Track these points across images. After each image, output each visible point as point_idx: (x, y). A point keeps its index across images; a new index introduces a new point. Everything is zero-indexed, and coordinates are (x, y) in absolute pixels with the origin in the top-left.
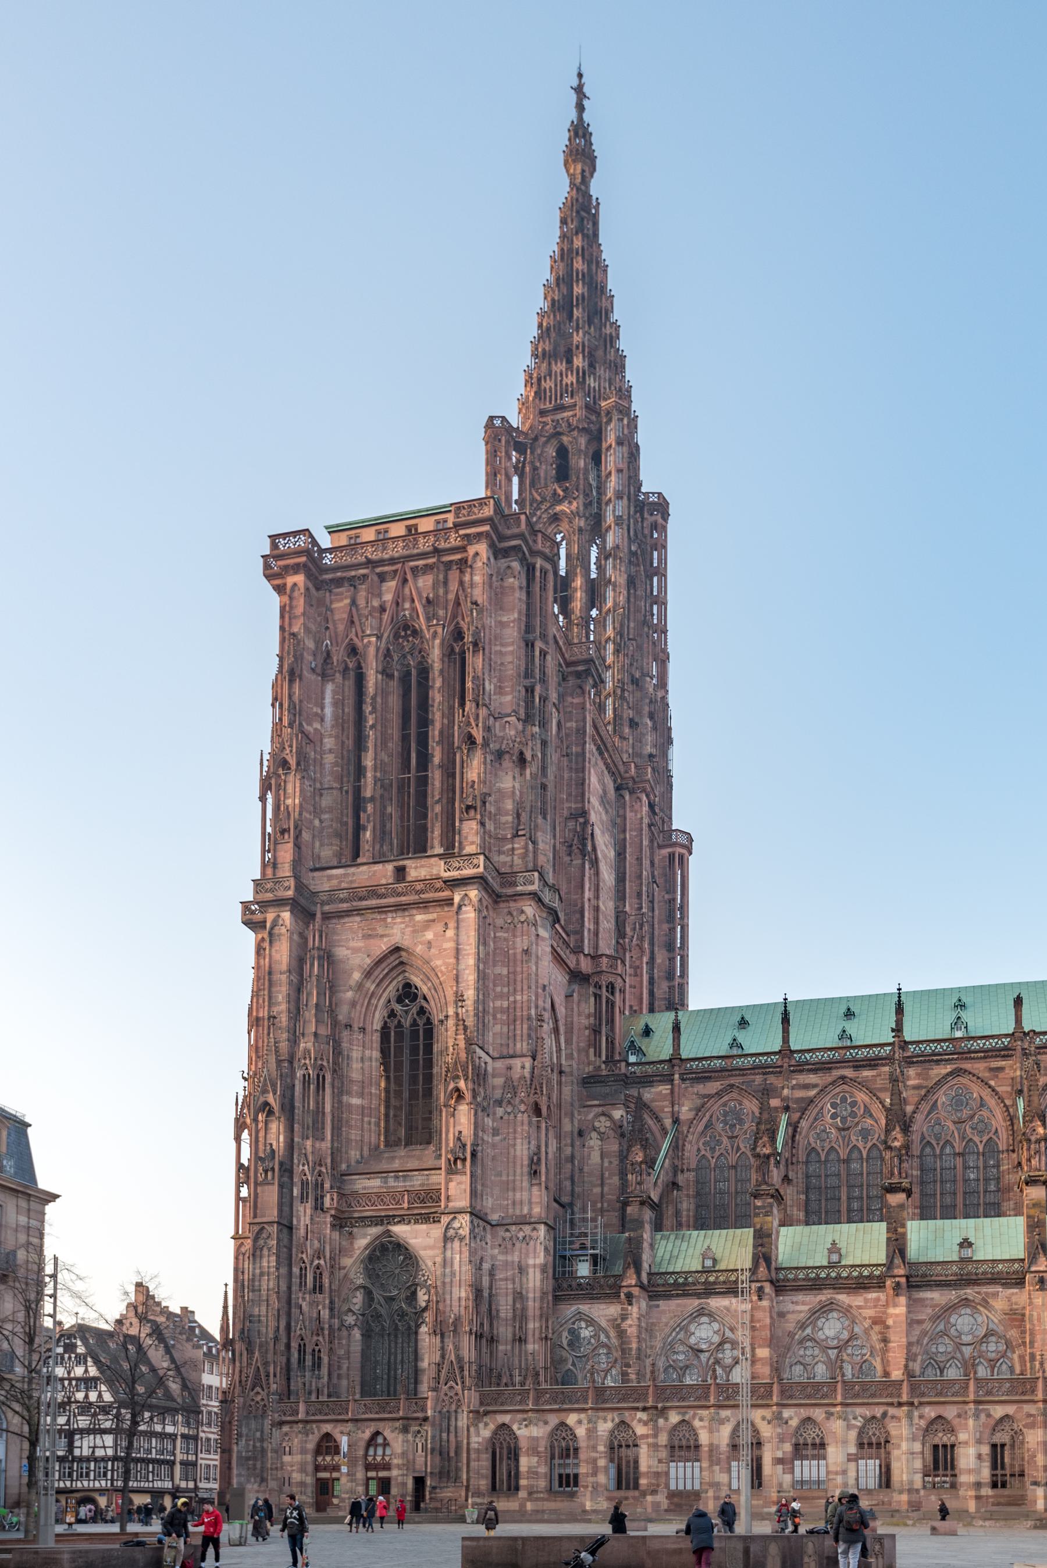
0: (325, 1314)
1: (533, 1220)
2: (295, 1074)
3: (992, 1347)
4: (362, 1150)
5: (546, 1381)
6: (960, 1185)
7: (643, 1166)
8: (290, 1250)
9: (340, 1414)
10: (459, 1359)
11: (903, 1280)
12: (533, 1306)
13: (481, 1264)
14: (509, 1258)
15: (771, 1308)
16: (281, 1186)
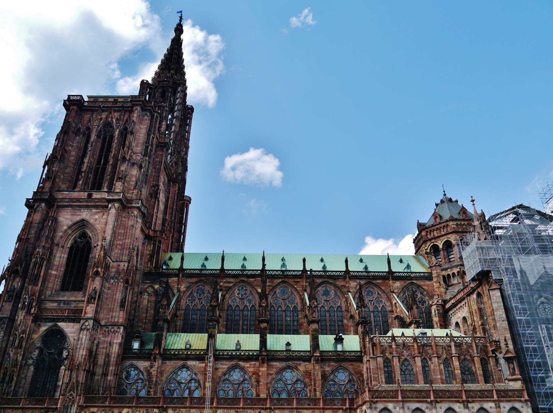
0: (20, 358)
1: (119, 324)
2: (32, 260)
3: (299, 386)
4: (52, 291)
5: (114, 394)
6: (284, 322)
7: (167, 306)
8: (11, 330)
9: (16, 405)
10: (77, 381)
11: (266, 357)
12: (113, 359)
13: (94, 341)
14: (106, 339)
15: (213, 366)
16: (14, 303)
